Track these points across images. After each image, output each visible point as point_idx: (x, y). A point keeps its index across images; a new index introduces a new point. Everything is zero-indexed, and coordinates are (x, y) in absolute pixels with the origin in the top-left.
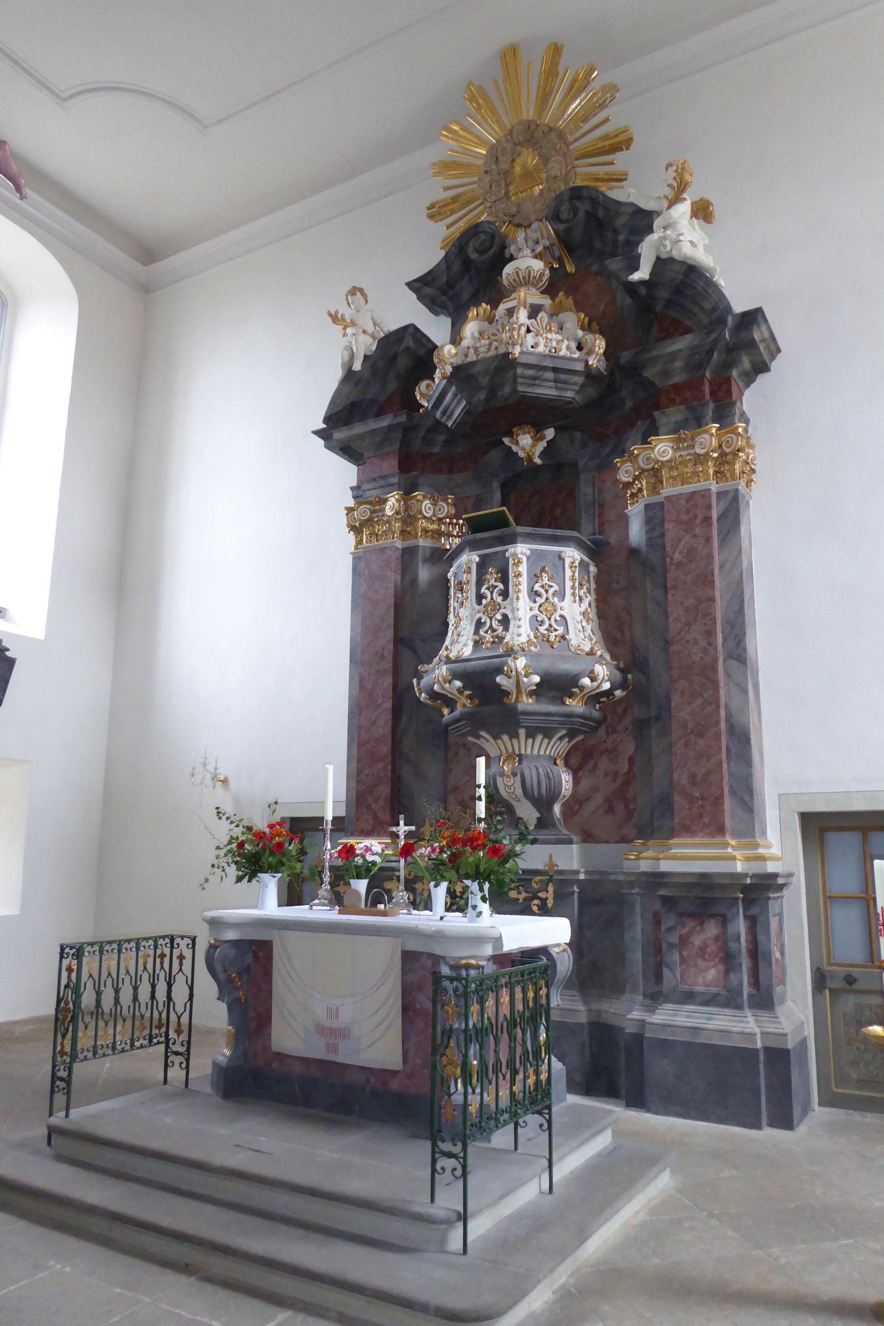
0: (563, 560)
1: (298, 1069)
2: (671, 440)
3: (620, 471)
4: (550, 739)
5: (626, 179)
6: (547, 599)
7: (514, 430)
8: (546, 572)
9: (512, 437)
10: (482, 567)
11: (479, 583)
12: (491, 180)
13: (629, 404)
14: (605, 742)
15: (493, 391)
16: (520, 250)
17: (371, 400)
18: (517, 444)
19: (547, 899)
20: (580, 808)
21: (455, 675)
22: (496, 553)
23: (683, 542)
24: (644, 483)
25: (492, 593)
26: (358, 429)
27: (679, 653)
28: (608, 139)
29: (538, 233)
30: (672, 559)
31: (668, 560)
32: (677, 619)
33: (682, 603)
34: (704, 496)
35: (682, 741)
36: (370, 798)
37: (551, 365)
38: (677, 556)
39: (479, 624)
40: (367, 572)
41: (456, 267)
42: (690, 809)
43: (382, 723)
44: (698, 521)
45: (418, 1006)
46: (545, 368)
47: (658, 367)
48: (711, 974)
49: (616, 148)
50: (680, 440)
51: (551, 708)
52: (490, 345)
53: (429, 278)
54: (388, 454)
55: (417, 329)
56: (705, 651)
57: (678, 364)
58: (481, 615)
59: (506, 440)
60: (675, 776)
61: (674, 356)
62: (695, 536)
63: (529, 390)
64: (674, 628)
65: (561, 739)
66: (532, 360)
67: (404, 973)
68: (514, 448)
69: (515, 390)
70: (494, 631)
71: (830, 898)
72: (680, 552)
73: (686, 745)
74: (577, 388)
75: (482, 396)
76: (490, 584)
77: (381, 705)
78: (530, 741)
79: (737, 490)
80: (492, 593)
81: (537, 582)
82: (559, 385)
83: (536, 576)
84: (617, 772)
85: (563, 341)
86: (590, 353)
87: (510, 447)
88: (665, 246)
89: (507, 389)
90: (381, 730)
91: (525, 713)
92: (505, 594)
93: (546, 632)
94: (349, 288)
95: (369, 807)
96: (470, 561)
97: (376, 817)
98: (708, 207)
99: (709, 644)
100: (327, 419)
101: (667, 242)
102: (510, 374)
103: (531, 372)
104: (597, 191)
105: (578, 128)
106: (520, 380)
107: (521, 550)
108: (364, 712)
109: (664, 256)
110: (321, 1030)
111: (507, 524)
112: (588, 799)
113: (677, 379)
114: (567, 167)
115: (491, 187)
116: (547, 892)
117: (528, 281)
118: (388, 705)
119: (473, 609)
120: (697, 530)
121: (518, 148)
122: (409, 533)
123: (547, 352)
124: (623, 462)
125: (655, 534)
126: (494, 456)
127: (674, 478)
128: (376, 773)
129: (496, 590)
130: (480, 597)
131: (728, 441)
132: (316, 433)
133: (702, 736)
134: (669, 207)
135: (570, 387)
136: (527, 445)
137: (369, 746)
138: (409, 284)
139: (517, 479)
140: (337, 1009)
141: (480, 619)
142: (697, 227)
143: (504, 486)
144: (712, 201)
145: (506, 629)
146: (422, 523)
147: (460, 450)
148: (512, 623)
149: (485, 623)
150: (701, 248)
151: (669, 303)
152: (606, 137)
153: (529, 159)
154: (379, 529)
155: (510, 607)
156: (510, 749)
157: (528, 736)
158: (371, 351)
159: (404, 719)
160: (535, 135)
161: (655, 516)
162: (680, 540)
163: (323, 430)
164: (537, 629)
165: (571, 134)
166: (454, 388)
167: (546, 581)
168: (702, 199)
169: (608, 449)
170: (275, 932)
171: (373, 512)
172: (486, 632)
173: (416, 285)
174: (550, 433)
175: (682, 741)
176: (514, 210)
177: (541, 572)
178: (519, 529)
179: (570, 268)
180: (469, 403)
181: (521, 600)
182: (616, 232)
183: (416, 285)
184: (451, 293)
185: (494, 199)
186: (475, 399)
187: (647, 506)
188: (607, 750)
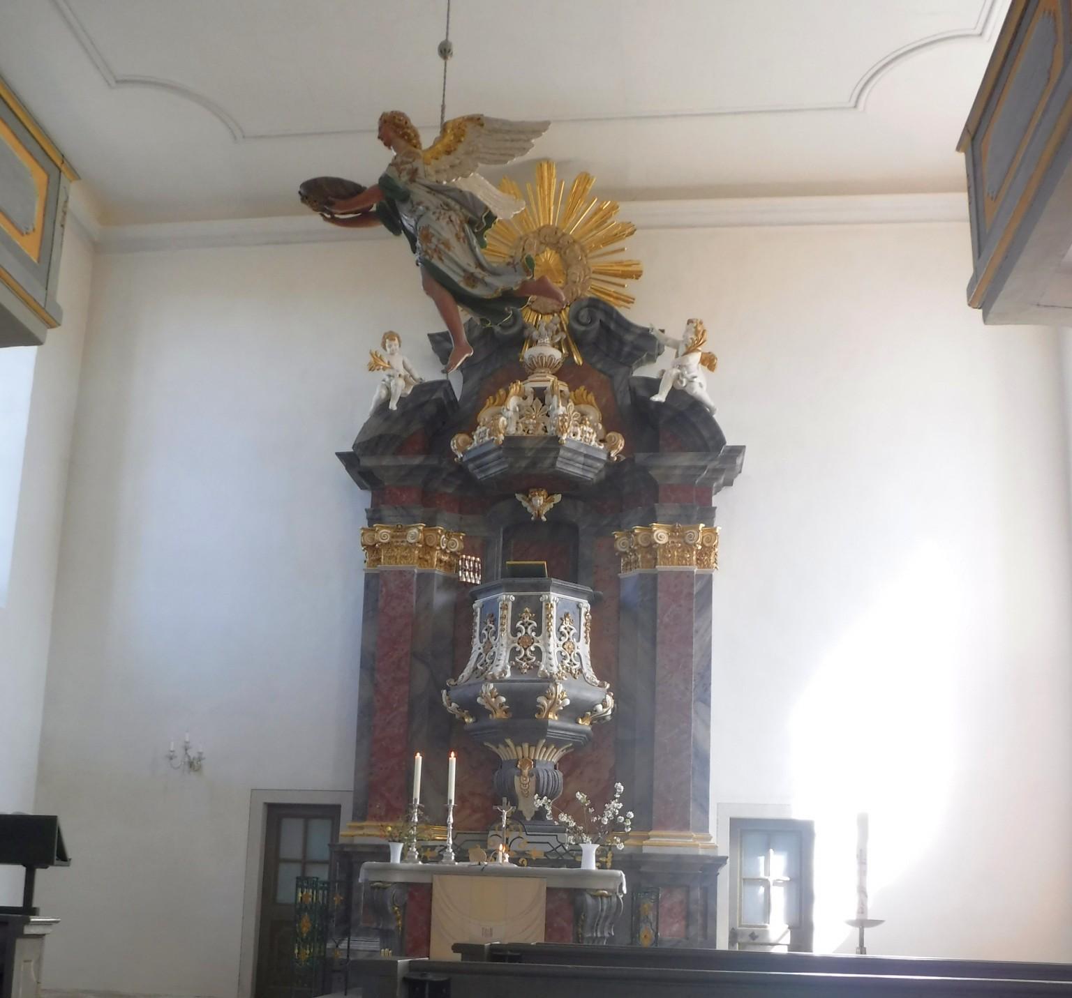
0: (580, 609)
2: (668, 529)
3: (618, 542)
5: (633, 303)
6: (569, 639)
8: (569, 618)
10: (518, 606)
11: (514, 621)
15: (534, 463)
16: (540, 335)
18: (530, 500)
19: (606, 862)
24: (640, 556)
25: (526, 628)
26: (387, 461)
28: (622, 265)
29: (558, 325)
31: (658, 621)
34: (688, 576)
37: (585, 452)
38: (666, 620)
45: (555, 925)
46: (580, 454)
48: (676, 928)
50: (673, 530)
51: (571, 726)
52: (538, 424)
55: (450, 385)
59: (519, 497)
62: (680, 606)
63: (564, 467)
65: (563, 751)
66: (573, 446)
67: (548, 902)
68: (525, 504)
69: (553, 465)
70: (530, 659)
71: (744, 879)
72: (668, 616)
74: (597, 471)
75: (523, 464)
76: (525, 621)
79: (711, 575)
80: (526, 628)
81: (562, 624)
82: (586, 467)
83: (561, 619)
85: (593, 433)
86: (613, 448)
88: (682, 382)
89: (548, 462)
91: (552, 727)
92: (538, 631)
93: (568, 665)
96: (508, 600)
98: (713, 360)
101: (684, 380)
103: (569, 455)
104: (612, 309)
105: (597, 248)
106: (559, 459)
107: (554, 596)
109: (678, 388)
111: (542, 575)
114: (585, 276)
116: (607, 857)
117: (548, 365)
118: (404, 709)
122: (427, 561)
123: (582, 442)
129: (530, 627)
130: (515, 631)
131: (708, 538)
132: (340, 455)
134: (686, 353)
135: (592, 470)
136: (540, 503)
138: (429, 335)
139: (521, 523)
140: (491, 930)
142: (700, 369)
143: (506, 531)
144: (717, 356)
145: (540, 659)
146: (436, 554)
148: (544, 655)
149: (520, 652)
150: (705, 388)
152: (620, 263)
154: (397, 552)
155: (543, 642)
158: (405, 394)
160: (561, 242)
163: (349, 454)
164: (562, 662)
165: (591, 251)
166: (501, 452)
167: (568, 625)
168: (709, 353)
169: (605, 522)
170: (436, 877)
171: (392, 537)
172: (521, 659)
173: (438, 338)
174: (558, 498)
177: (565, 617)
178: (554, 581)
179: (577, 359)
181: (552, 638)
183: (438, 338)
186: (517, 465)
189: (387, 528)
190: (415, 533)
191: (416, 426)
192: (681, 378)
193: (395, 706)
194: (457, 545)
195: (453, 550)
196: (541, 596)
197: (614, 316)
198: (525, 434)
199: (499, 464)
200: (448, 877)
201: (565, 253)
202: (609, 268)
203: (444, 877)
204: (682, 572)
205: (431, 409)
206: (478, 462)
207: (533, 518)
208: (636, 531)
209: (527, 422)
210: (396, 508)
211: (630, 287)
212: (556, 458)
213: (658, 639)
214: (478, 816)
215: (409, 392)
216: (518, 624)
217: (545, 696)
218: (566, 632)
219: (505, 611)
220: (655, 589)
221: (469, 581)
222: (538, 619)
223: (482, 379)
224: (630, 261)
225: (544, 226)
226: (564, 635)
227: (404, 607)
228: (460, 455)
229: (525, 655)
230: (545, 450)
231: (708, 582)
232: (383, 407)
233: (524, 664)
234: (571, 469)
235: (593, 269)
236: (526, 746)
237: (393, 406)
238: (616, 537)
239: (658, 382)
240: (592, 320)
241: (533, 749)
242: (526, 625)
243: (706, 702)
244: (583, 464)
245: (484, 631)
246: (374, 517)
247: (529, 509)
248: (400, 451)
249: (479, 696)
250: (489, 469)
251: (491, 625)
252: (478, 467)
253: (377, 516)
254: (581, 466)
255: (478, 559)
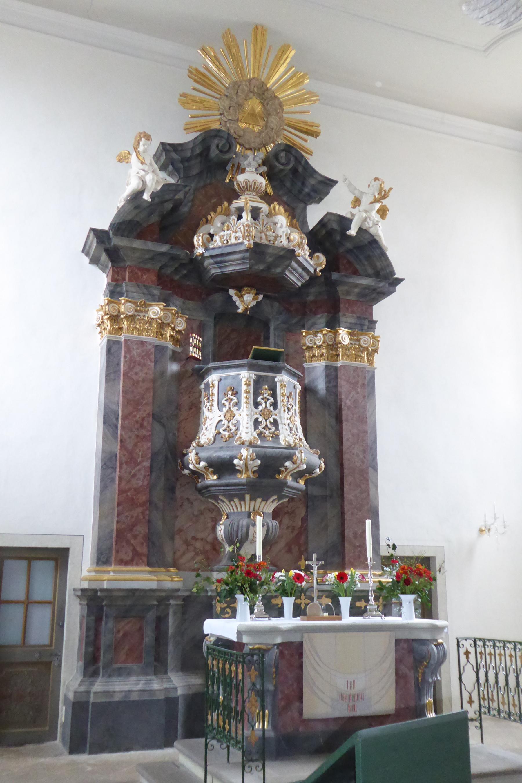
1: (320, 727)
4: (244, 500)
7: (246, 288)
9: (240, 292)
10: (258, 383)
12: (230, 104)
13: (311, 298)
14: (287, 507)
16: (249, 165)
17: (138, 222)
18: (241, 297)
20: (270, 549)
21: (258, 457)
22: (267, 376)
23: (351, 395)
25: (266, 403)
26: (138, 244)
27: (349, 460)
30: (345, 404)
32: (348, 440)
33: (351, 431)
35: (350, 512)
36: (129, 535)
39: (257, 423)
40: (128, 356)
41: (198, 151)
42: (354, 552)
43: (141, 477)
44: (359, 385)
47: (346, 288)
49: (312, 135)
53: (180, 148)
54: (148, 270)
56: (363, 462)
57: (357, 290)
58: (258, 416)
60: (346, 532)
61: (356, 286)
62: (358, 393)
64: (346, 444)
65: (273, 501)
68: (235, 298)
69: (283, 272)
70: (270, 429)
72: (350, 400)
73: (352, 514)
74: (304, 281)
75: (261, 267)
77: (140, 462)
78: (253, 503)
80: (266, 403)
82: (300, 278)
84: (294, 527)
87: (232, 297)
89: (278, 270)
90: (140, 483)
92: (275, 405)
94: (149, 133)
95: (128, 542)
97: (134, 550)
99: (364, 457)
100: (112, 226)
102: (288, 262)
108: (125, 466)
109: (364, 228)
110: (343, 697)
112: (276, 543)
113: (350, 298)
115: (229, 108)
118: (147, 464)
119: (252, 411)
120: (359, 390)
121: (251, 95)
124: (308, 334)
125: (331, 385)
126: (217, 298)
127: (348, 356)
128: (135, 515)
130: (257, 405)
133: (360, 511)
136: (245, 301)
137: (129, 494)
140: (354, 682)
141: (256, 420)
145: (277, 429)
147: (188, 283)
148: (280, 426)
151: (349, 251)
152: (305, 123)
153: (254, 105)
156: (256, 508)
157: (251, 500)
158: (156, 189)
159: (154, 475)
160: (266, 94)
161: (332, 374)
162: (350, 393)
163: (103, 232)
169: (294, 321)
170: (305, 635)
172: (264, 428)
174: (261, 297)
175: (350, 512)
176: (241, 133)
180: (250, 268)
182: (303, 184)
183: (168, 147)
184: (186, 164)
185: (230, 118)
186: (256, 267)
187: (327, 367)
188: (288, 512)
189: (131, 302)
190: (155, 311)
191: (155, 219)
192: (368, 220)
193: (139, 460)
194: (181, 325)
195: (180, 329)
196: (276, 377)
197: (303, 162)
198: (267, 243)
199: (240, 264)
200: (318, 635)
201: (268, 104)
202: (297, 124)
203: (311, 635)
204: (357, 367)
205: (169, 206)
206: (219, 259)
207: (240, 311)
208: (325, 332)
209: (268, 233)
210: (138, 286)
211: (310, 143)
212: (286, 267)
213: (344, 418)
214: (200, 558)
215: (159, 188)
216: (259, 399)
217: (292, 461)
218: (290, 407)
219: (249, 387)
220: (336, 377)
221: (196, 356)
222: (274, 395)
223: (196, 190)
224: (313, 123)
225: (254, 78)
226: (224, 405)
227: (146, 373)
228: (200, 250)
229: (266, 425)
230: (282, 257)
231: (373, 377)
232: (137, 195)
233: (267, 432)
234: (292, 277)
235: (286, 122)
236: (259, 500)
237: (146, 197)
238: (304, 334)
239: (350, 221)
240: (287, 164)
241: (264, 503)
242: (266, 400)
243: (375, 469)
244: (300, 275)
245: (223, 402)
246: (114, 293)
247: (238, 303)
248: (141, 236)
249: (236, 458)
250: (226, 266)
251: (232, 397)
252: (216, 263)
253: (118, 289)
254: (297, 275)
255: (201, 339)
